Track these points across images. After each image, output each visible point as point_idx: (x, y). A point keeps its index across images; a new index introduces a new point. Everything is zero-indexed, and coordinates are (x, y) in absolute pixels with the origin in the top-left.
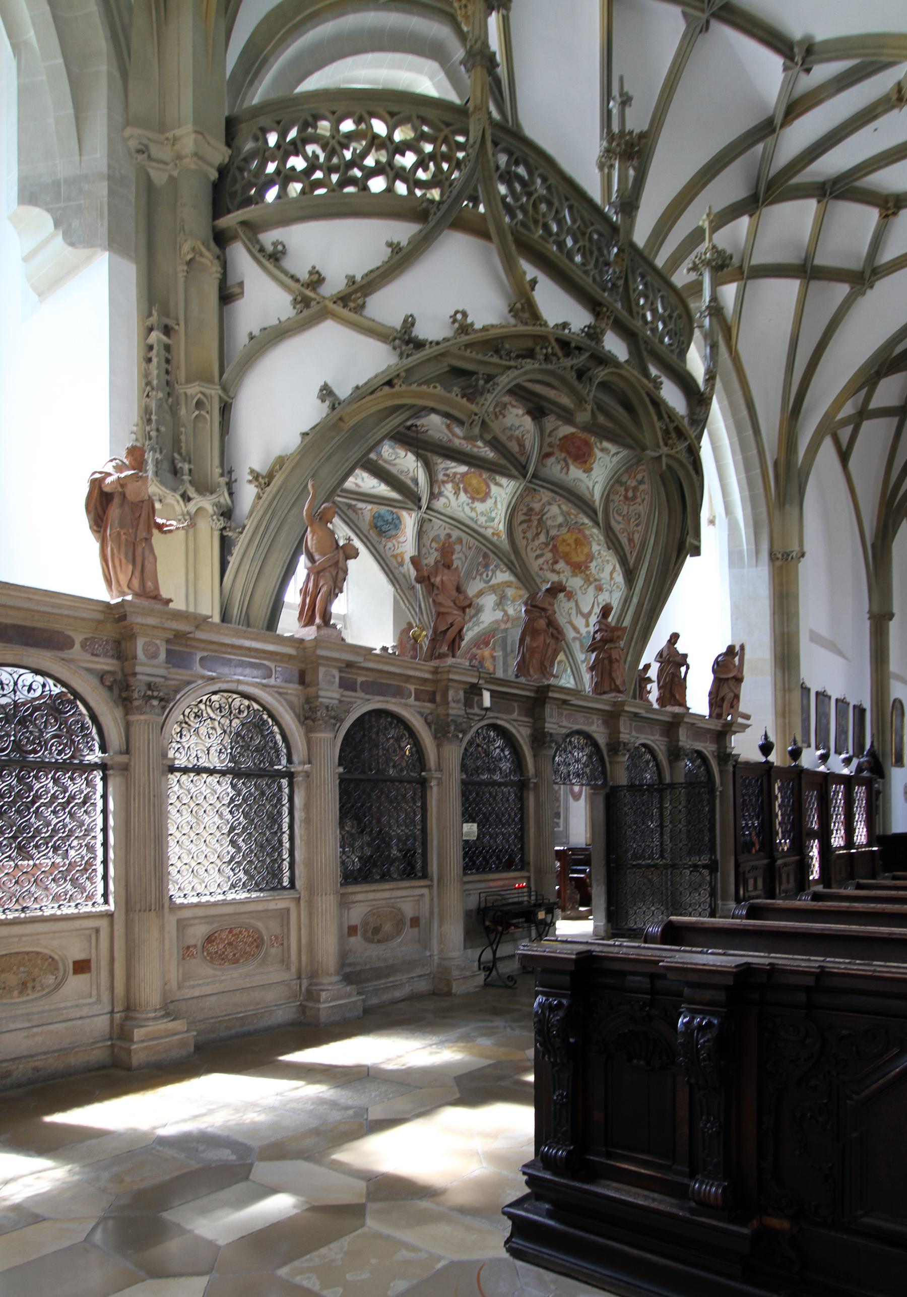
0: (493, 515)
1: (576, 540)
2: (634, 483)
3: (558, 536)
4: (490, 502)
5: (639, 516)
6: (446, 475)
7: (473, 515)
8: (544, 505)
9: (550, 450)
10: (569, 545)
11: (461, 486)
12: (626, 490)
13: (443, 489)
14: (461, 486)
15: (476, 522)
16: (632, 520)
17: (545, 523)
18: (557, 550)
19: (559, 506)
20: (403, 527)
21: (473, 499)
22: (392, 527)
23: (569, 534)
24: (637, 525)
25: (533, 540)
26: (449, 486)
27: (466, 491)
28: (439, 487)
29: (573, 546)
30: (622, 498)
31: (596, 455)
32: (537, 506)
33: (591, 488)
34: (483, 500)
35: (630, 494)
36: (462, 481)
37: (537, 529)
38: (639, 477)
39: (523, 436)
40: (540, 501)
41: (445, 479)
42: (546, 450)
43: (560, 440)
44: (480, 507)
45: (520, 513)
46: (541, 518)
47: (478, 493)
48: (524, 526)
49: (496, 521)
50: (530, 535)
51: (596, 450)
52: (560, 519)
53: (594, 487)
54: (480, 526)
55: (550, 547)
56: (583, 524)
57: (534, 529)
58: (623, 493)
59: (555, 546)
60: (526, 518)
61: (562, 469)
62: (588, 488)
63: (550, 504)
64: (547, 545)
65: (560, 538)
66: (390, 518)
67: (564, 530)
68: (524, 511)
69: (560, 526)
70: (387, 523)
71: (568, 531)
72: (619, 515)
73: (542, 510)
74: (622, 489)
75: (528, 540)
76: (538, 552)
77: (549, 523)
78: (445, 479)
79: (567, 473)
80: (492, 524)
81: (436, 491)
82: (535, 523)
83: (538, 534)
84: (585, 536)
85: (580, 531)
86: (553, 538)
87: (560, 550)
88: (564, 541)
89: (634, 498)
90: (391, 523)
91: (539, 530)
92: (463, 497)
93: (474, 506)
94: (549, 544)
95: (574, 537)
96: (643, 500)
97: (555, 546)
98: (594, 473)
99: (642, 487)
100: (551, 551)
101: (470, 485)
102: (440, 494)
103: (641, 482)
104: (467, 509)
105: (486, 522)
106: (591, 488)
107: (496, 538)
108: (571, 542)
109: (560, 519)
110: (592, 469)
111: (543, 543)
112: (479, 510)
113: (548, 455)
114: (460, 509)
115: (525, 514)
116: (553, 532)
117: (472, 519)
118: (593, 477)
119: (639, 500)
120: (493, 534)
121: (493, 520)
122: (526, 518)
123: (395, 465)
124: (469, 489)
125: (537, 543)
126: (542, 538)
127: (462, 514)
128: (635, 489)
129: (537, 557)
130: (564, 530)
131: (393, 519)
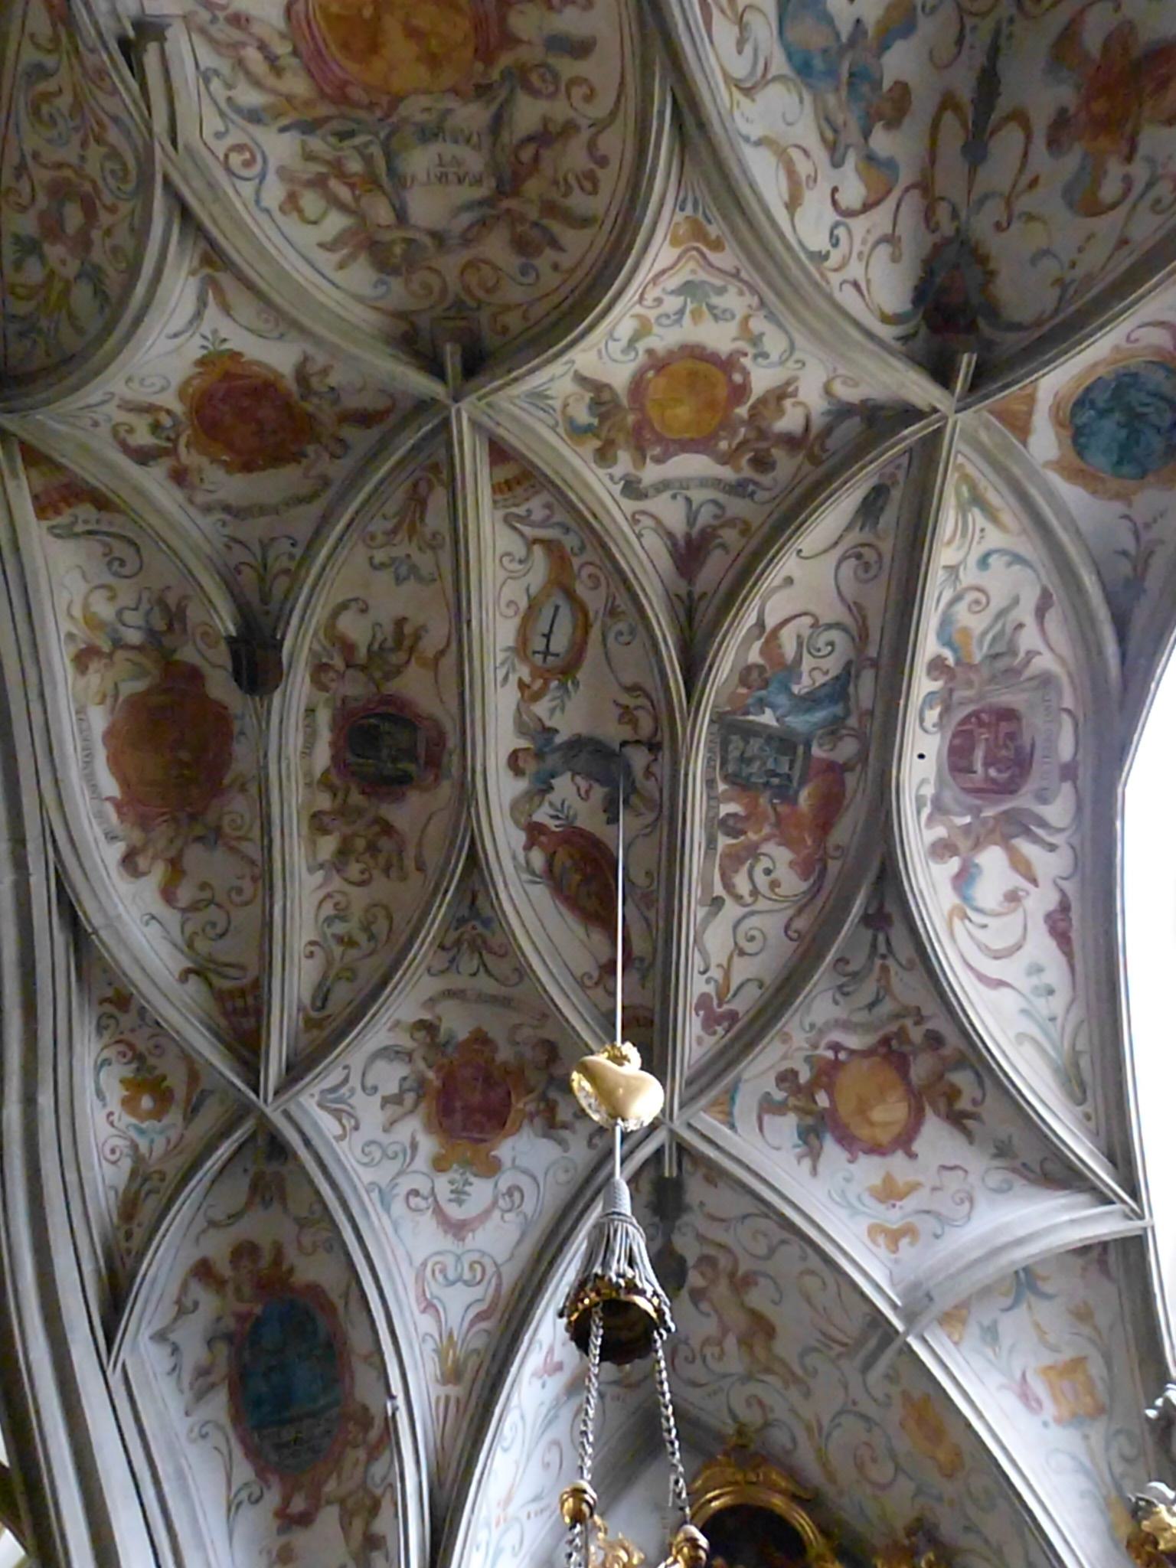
0: (672, 303)
1: (374, 47)
2: (55, 252)
3: (455, 91)
4: (664, 339)
5: (36, 112)
6: (762, 463)
7: (758, 324)
8: (467, 240)
9: (349, 433)
10: (413, 33)
11: (742, 411)
12: (84, 243)
13: (817, 423)
14: (742, 411)
15: (762, 303)
16: (64, 102)
17: (494, 168)
18: (479, 25)
19: (401, 217)
20: (1101, 371)
21: (727, 364)
22: (1135, 397)
23: (397, 84)
24: (40, 72)
25: (569, 128)
26: (790, 421)
27: (740, 392)
28: (828, 430)
29: (392, 26)
30: (105, 219)
31: (181, 394)
32: (496, 247)
33: (212, 311)
34: (695, 353)
35: (74, 217)
36: (727, 425)
37: (536, 158)
38: (33, 272)
39: (394, 531)
40: (471, 265)
41: (778, 453)
42: (360, 439)
43: (297, 457)
44: (719, 338)
45: (566, 261)
46: (500, 192)
47: (693, 374)
48: (579, 202)
49: (673, 282)
50: (574, 157)
51: (178, 408)
52: (419, 161)
53: (198, 315)
54: (753, 290)
55: (505, 60)
56: (308, 127)
57: (546, 165)
58: (96, 235)
59: (486, 54)
60: (556, 227)
61: (325, 371)
62: (226, 309)
63: (438, 237)
64: (520, 77)
65: (449, 76)
66: (1109, 425)
67: (414, 109)
68: (549, 254)
69: (429, 134)
70: (1134, 420)
71: (397, 100)
72: (114, 154)
73: (483, 223)
74: (97, 255)
75: (592, 146)
76: (568, 68)
77: (474, 161)
78: (778, 453)
79: (306, 359)
80: (702, 276)
81: (852, 426)
82: (533, 187)
83: (545, 137)
84: (314, 62)
85: (340, 96)
86: (483, 91)
87: (465, 25)
88: (433, 61)
89: (60, 191)
90: (1129, 410)
91: (527, 155)
92: (762, 379)
93: (742, 345)
94: (507, 74)
95: (378, 65)
96: (21, 169)
97: (486, 54)
98: (194, 349)
99: (27, 225)
100: (510, 40)
101: (711, 405)
102: (842, 411)
103: (30, 247)
104: (774, 343)
105: (721, 291)
106: (212, 311)
107: (713, 231)
108: (398, 46)
109: (419, 161)
110: (201, 362)
111: (535, 93)
112: (732, 328)
113: (365, 419)
114: (797, 355)
115: (555, 244)
116: (472, 115)
117: (771, 317)
118: (198, 341)
119: (42, 176)
120: (717, 245)
121: (687, 289)
122: (556, 227)
123: (856, 609)
124: (722, 392)
125: (560, 110)
126: (528, 114)
127: (799, 340)
128: (53, 228)
129: (581, 49)
130: (414, 109)
131: (1103, 413)
